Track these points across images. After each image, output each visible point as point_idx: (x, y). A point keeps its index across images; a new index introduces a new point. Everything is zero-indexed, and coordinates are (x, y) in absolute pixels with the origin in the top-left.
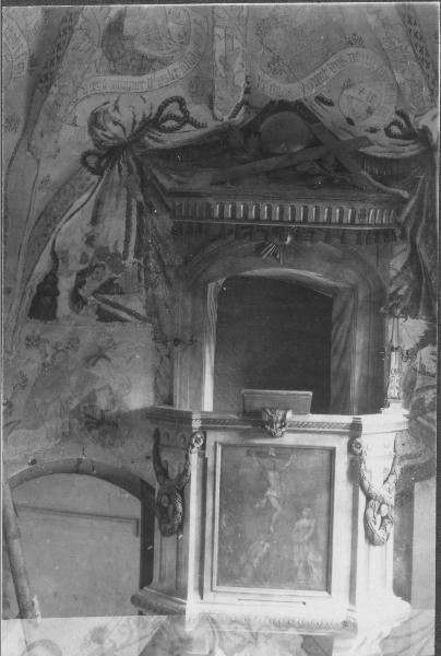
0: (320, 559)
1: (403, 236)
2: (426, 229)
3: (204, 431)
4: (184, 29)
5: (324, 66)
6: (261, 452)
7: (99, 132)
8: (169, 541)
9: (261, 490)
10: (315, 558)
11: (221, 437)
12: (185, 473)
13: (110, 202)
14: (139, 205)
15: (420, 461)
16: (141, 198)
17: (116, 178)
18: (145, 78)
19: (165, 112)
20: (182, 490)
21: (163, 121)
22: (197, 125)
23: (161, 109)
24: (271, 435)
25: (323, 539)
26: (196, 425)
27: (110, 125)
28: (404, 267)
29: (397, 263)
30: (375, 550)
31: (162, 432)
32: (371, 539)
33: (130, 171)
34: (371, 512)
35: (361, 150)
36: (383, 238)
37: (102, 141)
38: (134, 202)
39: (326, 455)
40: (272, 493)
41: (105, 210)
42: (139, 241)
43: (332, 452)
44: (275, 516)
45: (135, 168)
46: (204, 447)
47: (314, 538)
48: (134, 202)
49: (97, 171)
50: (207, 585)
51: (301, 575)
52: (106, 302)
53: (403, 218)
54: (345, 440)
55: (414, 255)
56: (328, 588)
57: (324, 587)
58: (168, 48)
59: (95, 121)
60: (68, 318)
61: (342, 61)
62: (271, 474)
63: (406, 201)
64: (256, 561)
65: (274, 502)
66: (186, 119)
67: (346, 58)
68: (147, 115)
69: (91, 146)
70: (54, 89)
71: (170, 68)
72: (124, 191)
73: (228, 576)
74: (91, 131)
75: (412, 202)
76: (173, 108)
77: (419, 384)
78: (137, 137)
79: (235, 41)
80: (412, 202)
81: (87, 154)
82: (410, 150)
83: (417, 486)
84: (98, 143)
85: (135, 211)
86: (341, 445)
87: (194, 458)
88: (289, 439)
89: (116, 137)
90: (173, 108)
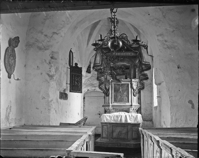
0: (127, 98)
1: (138, 58)
2: (141, 56)
3: (111, 82)
6: (119, 85)
8: (107, 97)
10: (127, 98)
11: (114, 83)
12: (109, 88)
13: (98, 55)
14: (102, 55)
20: (109, 90)
24: (120, 82)
26: (110, 81)
28: (138, 62)
29: (137, 61)
30: (135, 97)
31: (106, 84)
32: (134, 95)
33: (100, 51)
36: (135, 57)
39: (127, 85)
40: (121, 90)
46: (111, 84)
47: (126, 96)
49: (96, 51)
50: (112, 102)
51: (125, 100)
54: (130, 82)
55: (139, 60)
57: (128, 102)
60: (92, 71)
62: (120, 87)
63: (138, 53)
65: (121, 91)
72: (99, 53)
73: (115, 101)
77: (141, 77)
81: (95, 48)
82: (137, 46)
83: (141, 91)
85: (101, 56)
86: (129, 83)
87: (110, 85)
88: (123, 83)
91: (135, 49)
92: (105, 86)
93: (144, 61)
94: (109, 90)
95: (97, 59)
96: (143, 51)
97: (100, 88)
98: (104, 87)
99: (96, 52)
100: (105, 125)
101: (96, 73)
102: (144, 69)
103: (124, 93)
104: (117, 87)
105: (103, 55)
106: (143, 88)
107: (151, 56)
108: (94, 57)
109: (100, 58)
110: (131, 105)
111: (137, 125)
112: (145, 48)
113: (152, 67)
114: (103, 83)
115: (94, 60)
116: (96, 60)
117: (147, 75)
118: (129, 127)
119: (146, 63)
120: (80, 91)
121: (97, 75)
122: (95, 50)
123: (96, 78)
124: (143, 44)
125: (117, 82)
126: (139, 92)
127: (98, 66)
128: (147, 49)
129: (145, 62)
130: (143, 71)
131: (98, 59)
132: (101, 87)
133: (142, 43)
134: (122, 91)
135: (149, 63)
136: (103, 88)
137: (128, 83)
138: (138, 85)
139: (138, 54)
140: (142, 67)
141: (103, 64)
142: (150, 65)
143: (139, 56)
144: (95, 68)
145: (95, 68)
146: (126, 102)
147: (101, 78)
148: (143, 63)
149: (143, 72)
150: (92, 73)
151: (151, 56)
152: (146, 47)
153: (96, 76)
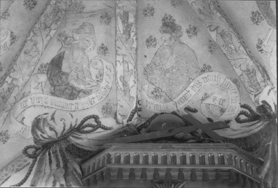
4: (99, 72)
5: (188, 89)
7: (39, 133)
16: (63, 182)
17: (48, 170)
18: (74, 102)
21: (83, 128)
22: (105, 128)
23: (83, 122)
27: (47, 129)
33: (58, 166)
37: (40, 140)
45: (62, 165)
49: (34, 156)
58: (89, 84)
59: (37, 124)
61: (199, 83)
67: (202, 81)
68: (73, 125)
69: (32, 143)
70: (8, 80)
71: (90, 97)
72: (52, 179)
74: (33, 131)
78: (64, 137)
79: (130, 65)
84: (36, 141)
89: (50, 137)
90: (92, 121)
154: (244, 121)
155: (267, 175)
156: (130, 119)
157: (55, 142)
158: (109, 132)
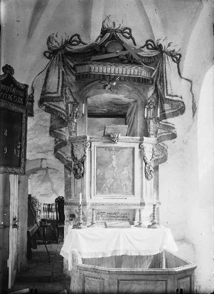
2: (160, 80)
6: (110, 149)
7: (50, 44)
9: (111, 162)
14: (63, 72)
15: (161, 157)
19: (73, 39)
22: (84, 44)
23: (71, 38)
24: (114, 142)
25: (131, 177)
27: (54, 42)
28: (153, 95)
33: (59, 60)
34: (147, 168)
35: (139, 53)
38: (61, 71)
39: (131, 150)
40: (114, 163)
41: (50, 73)
42: (63, 84)
43: (134, 149)
44: (115, 170)
45: (61, 60)
46: (90, 147)
48: (61, 71)
49: (48, 58)
50: (92, 194)
52: (51, 104)
53: (152, 76)
54: (138, 144)
55: (156, 90)
56: (134, 194)
62: (113, 156)
63: (154, 71)
64: (109, 186)
65: (115, 166)
66: (80, 42)
68: (67, 39)
69: (46, 49)
72: (57, 68)
73: (99, 189)
74: (48, 44)
75: (155, 72)
76: (76, 38)
78: (63, 47)
80: (155, 72)
81: (45, 52)
82: (155, 53)
84: (49, 48)
86: (136, 146)
87: (87, 150)
89: (55, 47)
90: (76, 38)
91: (149, 61)
92: (72, 152)
93: (169, 92)
94: (83, 163)
95: (50, 81)
96: (170, 66)
97: (58, 157)
98: (70, 155)
99: (49, 60)
100: (94, 274)
101: (48, 116)
102: (167, 112)
103: (123, 170)
104: (106, 154)
105: (66, 72)
106: (164, 159)
107: (187, 80)
108: (43, 76)
109: (59, 78)
110: (142, 204)
111: (188, 273)
112: (173, 60)
113: (188, 110)
114: (64, 143)
115: (42, 83)
116: (48, 84)
117: (174, 128)
118: (169, 282)
119: (174, 98)
120: (19, 166)
121: (51, 121)
122: (47, 57)
123: (48, 129)
124: (170, 49)
125: (105, 142)
126: (156, 168)
127: (52, 99)
128: (178, 62)
129: (170, 95)
130: (164, 116)
131: (54, 79)
132: (59, 152)
133: (169, 45)
134: (117, 165)
135: (180, 99)
136: (65, 157)
137: (132, 145)
138: (156, 153)
139: (154, 74)
140: (162, 108)
141: (66, 93)
142: (183, 103)
143: (157, 80)
144: (45, 103)
145: (45, 103)
146: (127, 193)
147: (61, 131)
148: (167, 97)
149: (164, 121)
150: (36, 115)
151: (187, 80)
152: (176, 58)
153: (48, 124)
154: (150, 49)
155: (154, 76)
156: (97, 39)
157: (58, 50)
158: (85, 46)
